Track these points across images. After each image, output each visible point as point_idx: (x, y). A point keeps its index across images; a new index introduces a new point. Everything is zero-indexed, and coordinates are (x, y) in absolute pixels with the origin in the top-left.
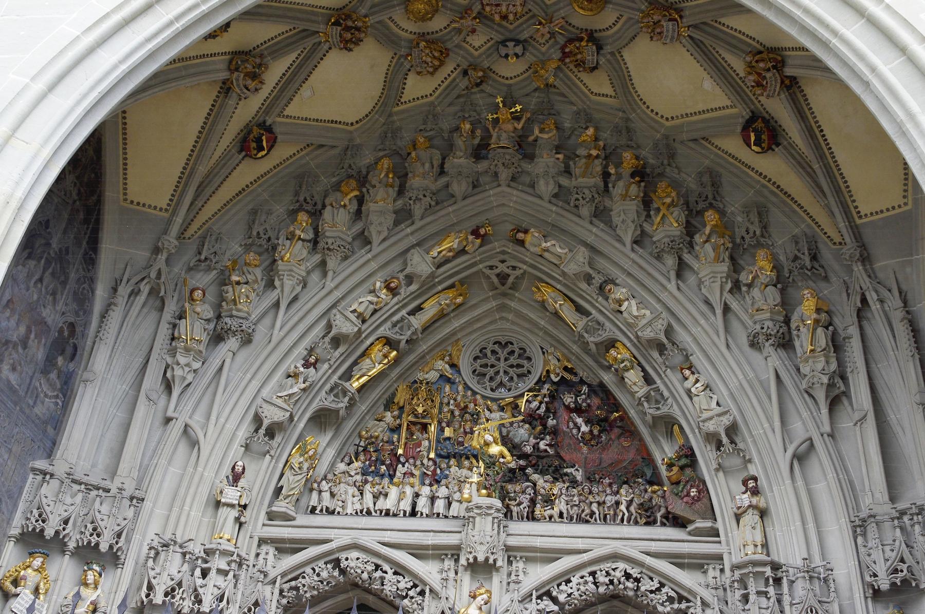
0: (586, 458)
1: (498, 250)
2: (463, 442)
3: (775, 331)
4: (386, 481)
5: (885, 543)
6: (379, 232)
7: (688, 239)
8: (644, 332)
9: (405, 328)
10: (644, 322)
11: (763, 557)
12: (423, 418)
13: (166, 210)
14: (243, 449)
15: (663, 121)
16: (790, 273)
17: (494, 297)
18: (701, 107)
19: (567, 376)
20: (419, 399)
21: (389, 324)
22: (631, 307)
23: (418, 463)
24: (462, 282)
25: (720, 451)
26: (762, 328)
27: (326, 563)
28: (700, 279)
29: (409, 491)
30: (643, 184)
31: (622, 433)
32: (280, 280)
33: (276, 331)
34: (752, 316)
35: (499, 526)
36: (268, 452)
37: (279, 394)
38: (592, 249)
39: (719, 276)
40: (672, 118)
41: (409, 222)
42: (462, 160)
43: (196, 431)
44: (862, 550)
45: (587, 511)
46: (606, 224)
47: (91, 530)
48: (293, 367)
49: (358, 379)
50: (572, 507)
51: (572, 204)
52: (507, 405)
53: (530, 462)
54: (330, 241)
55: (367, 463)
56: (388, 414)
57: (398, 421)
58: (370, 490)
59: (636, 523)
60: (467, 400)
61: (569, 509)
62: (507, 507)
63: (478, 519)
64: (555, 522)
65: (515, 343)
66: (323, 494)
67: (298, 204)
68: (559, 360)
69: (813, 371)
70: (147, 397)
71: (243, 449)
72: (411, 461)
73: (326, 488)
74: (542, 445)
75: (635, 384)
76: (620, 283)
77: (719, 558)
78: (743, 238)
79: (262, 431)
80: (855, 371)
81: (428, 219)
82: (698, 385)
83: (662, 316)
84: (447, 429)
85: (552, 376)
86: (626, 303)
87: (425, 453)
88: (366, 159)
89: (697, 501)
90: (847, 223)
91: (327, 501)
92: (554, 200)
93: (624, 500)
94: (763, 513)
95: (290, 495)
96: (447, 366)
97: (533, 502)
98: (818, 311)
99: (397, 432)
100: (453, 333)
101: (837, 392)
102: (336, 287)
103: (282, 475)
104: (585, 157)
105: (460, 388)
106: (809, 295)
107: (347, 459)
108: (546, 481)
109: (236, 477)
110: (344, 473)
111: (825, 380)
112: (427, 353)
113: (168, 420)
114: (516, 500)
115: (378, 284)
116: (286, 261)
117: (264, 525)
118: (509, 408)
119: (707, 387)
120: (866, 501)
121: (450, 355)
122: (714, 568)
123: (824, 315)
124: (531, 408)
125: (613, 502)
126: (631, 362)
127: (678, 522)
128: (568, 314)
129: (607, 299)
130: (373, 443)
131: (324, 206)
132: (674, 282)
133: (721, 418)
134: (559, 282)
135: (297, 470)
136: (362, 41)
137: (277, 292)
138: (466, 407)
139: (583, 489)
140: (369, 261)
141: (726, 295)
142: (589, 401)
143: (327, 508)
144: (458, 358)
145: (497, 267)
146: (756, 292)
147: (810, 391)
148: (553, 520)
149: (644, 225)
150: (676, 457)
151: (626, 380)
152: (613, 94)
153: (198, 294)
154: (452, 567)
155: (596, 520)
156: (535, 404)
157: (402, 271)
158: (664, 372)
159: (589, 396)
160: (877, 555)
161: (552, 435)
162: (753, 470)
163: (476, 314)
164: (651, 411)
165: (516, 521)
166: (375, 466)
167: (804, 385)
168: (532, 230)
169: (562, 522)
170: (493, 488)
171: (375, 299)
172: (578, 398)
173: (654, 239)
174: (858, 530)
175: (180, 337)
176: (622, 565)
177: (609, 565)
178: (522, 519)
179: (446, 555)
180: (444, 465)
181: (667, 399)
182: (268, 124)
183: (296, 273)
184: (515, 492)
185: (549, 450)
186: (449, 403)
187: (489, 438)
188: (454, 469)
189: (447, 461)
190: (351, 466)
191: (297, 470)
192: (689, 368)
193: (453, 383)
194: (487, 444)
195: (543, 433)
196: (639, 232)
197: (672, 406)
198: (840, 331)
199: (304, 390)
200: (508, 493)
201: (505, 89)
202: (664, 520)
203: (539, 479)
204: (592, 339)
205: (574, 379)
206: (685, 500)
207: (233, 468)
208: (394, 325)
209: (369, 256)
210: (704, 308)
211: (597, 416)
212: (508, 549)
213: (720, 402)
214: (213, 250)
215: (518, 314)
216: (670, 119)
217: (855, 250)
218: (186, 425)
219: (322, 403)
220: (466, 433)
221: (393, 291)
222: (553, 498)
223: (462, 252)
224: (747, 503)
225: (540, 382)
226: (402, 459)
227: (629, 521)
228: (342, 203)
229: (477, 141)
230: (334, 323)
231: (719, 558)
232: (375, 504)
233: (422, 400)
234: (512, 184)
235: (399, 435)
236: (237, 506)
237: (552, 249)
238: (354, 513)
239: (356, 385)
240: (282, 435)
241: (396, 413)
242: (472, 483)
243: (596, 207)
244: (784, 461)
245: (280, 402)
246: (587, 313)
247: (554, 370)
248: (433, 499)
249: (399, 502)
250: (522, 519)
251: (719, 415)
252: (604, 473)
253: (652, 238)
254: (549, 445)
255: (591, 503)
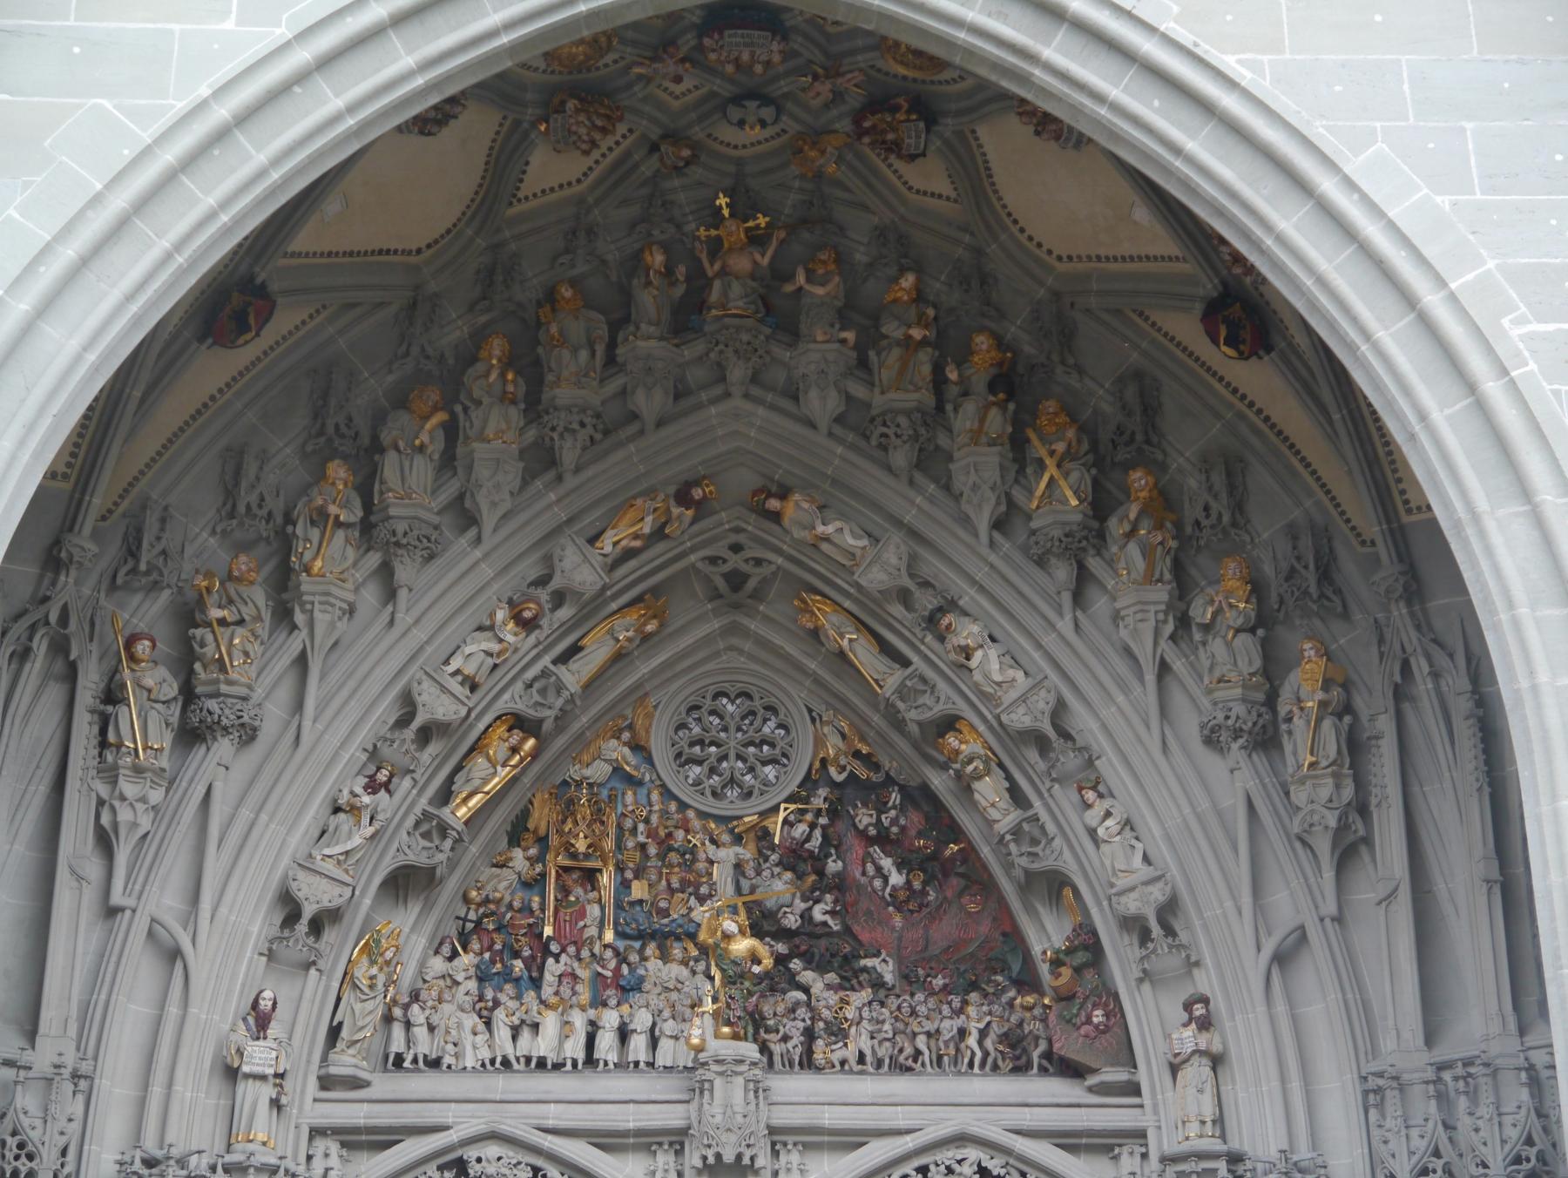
0: (900, 939)
1: (727, 526)
2: (667, 910)
3: (1250, 724)
4: (530, 996)
5: (1411, 1123)
6: (494, 504)
7: (1095, 524)
8: (1013, 716)
9: (551, 693)
10: (1013, 695)
11: (1217, 1146)
12: (587, 856)
13: (65, 476)
14: (264, 959)
15: (1052, 261)
16: (1281, 602)
17: (716, 613)
18: (1126, 249)
19: (863, 773)
20: (576, 823)
21: (519, 685)
22: (989, 663)
23: (585, 953)
24: (655, 591)
25: (1147, 948)
26: (1227, 718)
27: (441, 1168)
28: (1118, 611)
29: (579, 1020)
30: (1011, 406)
31: (966, 888)
32: (303, 611)
33: (307, 723)
34: (1209, 692)
35: (756, 1092)
36: (314, 963)
37: (327, 851)
38: (914, 534)
39: (1152, 608)
40: (1070, 258)
41: (551, 475)
42: (653, 343)
43: (173, 931)
44: (1375, 1132)
45: (909, 1050)
46: (936, 480)
47: (15, 1150)
48: (346, 792)
49: (465, 801)
50: (880, 1043)
51: (874, 442)
52: (746, 831)
53: (797, 947)
54: (401, 527)
55: (487, 955)
56: (518, 853)
57: (539, 868)
58: (506, 1020)
59: (995, 1067)
60: (669, 823)
61: (876, 1047)
62: (764, 1049)
63: (718, 1082)
64: (851, 1072)
65: (756, 696)
66: (415, 1030)
67: (322, 440)
68: (843, 736)
69: (1312, 802)
70: (73, 871)
71: (264, 959)
72: (572, 949)
73: (422, 1019)
74: (818, 914)
75: (993, 805)
76: (968, 608)
77: (1141, 1135)
78: (1197, 523)
79: (302, 927)
80: (1384, 805)
81: (589, 472)
82: (1109, 822)
83: (1046, 683)
84: (636, 885)
85: (833, 771)
86: (979, 654)
87: (592, 931)
88: (453, 332)
89: (1104, 1032)
90: (1385, 527)
91: (424, 1045)
92: (838, 430)
93: (974, 1027)
94: (1217, 1061)
95: (358, 1041)
96: (626, 750)
97: (810, 1035)
98: (1327, 685)
99: (536, 890)
100: (638, 685)
101: (1351, 838)
102: (417, 621)
103: (339, 999)
104: (898, 343)
105: (655, 796)
106: (1312, 653)
107: (446, 950)
108: (829, 987)
109: (261, 1021)
110: (443, 977)
111: (1332, 820)
112: (587, 728)
113: (111, 912)
114: (777, 1031)
115: (500, 615)
116: (317, 575)
117: (315, 1100)
118: (752, 835)
119: (1128, 824)
120: (1388, 1044)
121: (631, 727)
122: (1131, 1153)
123: (1336, 692)
124: (793, 839)
125: (955, 1030)
126: (987, 762)
127: (1072, 1070)
128: (865, 656)
129: (942, 639)
130: (493, 914)
131: (377, 448)
132: (1068, 617)
133: (1150, 888)
134: (847, 595)
135: (366, 990)
136: (455, 117)
137: (303, 634)
138: (670, 835)
139: (899, 1008)
140: (476, 564)
141: (1165, 646)
142: (902, 821)
143: (425, 1056)
144: (648, 732)
145: (725, 561)
146: (1217, 646)
147: (1305, 836)
148: (847, 1067)
149: (1014, 492)
150: (1067, 947)
151: (977, 796)
152: (953, 195)
153: (143, 647)
154: (672, 1164)
155: (923, 1065)
156: (800, 830)
157: (542, 581)
158: (1049, 790)
159: (902, 809)
160: (1397, 1145)
161: (836, 892)
162: (1204, 982)
163: (682, 647)
164: (1024, 861)
165: (780, 1072)
166: (502, 961)
167: (1296, 828)
168: (797, 497)
169: (862, 1073)
170: (742, 1023)
171: (495, 647)
172: (883, 817)
173: (1034, 525)
174: (1371, 1096)
175: (120, 745)
176: (973, 1154)
177: (950, 1154)
178: (791, 1065)
179: (660, 1144)
180: (634, 958)
181: (1053, 839)
182: (259, 280)
183: (336, 598)
184: (775, 1014)
185: (831, 922)
186: (635, 828)
187: (730, 926)
188: (654, 964)
189: (637, 945)
190: (456, 962)
191: (366, 990)
192: (1094, 788)
193: (640, 783)
194: (727, 937)
195: (819, 889)
196: (1003, 508)
197: (1061, 853)
198: (1364, 719)
199: (373, 837)
200: (764, 1018)
201: (732, 169)
202: (1045, 1063)
203: (814, 980)
204: (913, 715)
205: (876, 778)
206: (1082, 1031)
207: (255, 1005)
208: (529, 686)
209: (478, 553)
210: (1122, 667)
211: (920, 848)
212: (772, 1131)
213: (1152, 854)
214: (159, 548)
215: (762, 643)
216: (1065, 259)
217: (1397, 580)
218: (153, 920)
219: (402, 857)
220: (671, 891)
221: (527, 625)
222: (845, 1026)
223: (659, 534)
224: (1189, 1047)
225: (809, 782)
226: (554, 948)
227: (983, 1064)
228: (417, 442)
229: (679, 291)
230: (419, 700)
231: (1141, 1135)
232: (514, 1038)
233: (582, 826)
234: (756, 391)
235: (543, 897)
236: (271, 1078)
237: (837, 539)
238: (478, 1066)
239: (462, 812)
240: (336, 927)
241: (533, 851)
242: (704, 1013)
243: (921, 450)
244: (1255, 966)
245: (329, 867)
246: (905, 663)
247: (836, 759)
248: (624, 1034)
249: (561, 1044)
250: (791, 1065)
251: (1147, 883)
252: (933, 964)
253: (1029, 518)
254: (832, 913)
255: (915, 1035)
